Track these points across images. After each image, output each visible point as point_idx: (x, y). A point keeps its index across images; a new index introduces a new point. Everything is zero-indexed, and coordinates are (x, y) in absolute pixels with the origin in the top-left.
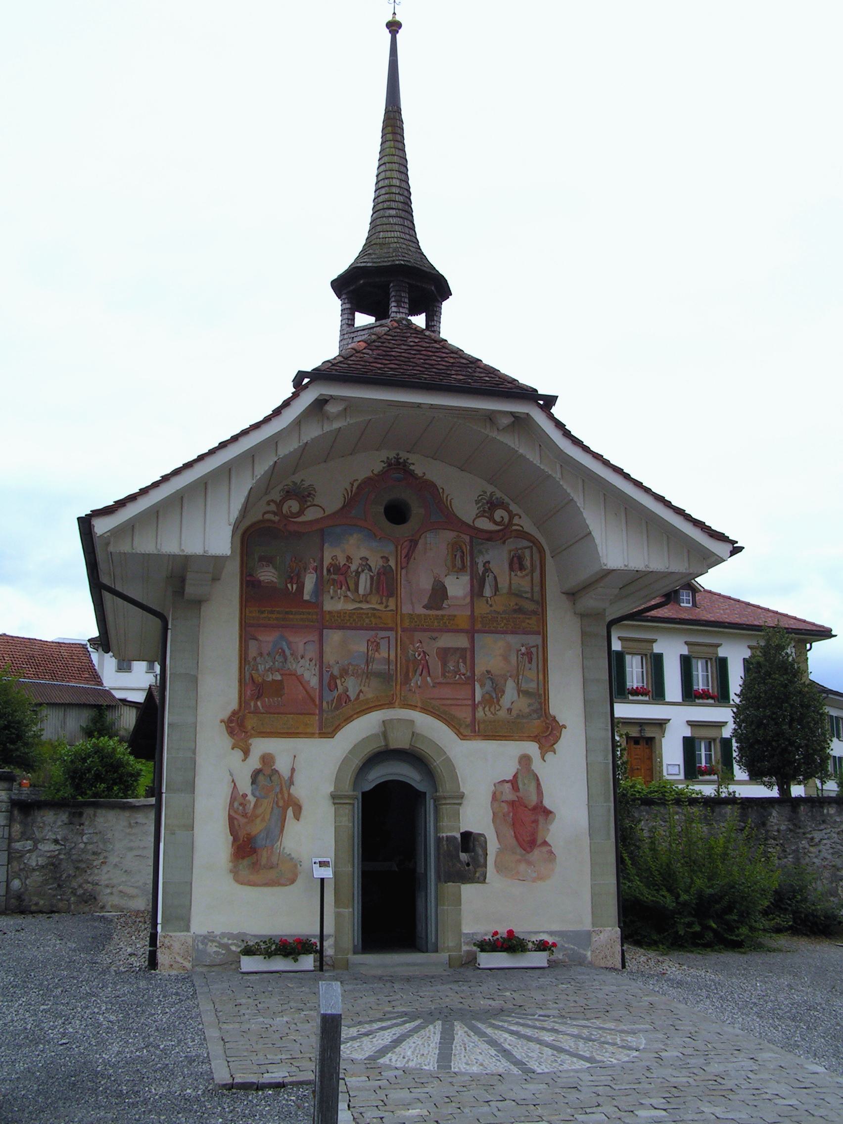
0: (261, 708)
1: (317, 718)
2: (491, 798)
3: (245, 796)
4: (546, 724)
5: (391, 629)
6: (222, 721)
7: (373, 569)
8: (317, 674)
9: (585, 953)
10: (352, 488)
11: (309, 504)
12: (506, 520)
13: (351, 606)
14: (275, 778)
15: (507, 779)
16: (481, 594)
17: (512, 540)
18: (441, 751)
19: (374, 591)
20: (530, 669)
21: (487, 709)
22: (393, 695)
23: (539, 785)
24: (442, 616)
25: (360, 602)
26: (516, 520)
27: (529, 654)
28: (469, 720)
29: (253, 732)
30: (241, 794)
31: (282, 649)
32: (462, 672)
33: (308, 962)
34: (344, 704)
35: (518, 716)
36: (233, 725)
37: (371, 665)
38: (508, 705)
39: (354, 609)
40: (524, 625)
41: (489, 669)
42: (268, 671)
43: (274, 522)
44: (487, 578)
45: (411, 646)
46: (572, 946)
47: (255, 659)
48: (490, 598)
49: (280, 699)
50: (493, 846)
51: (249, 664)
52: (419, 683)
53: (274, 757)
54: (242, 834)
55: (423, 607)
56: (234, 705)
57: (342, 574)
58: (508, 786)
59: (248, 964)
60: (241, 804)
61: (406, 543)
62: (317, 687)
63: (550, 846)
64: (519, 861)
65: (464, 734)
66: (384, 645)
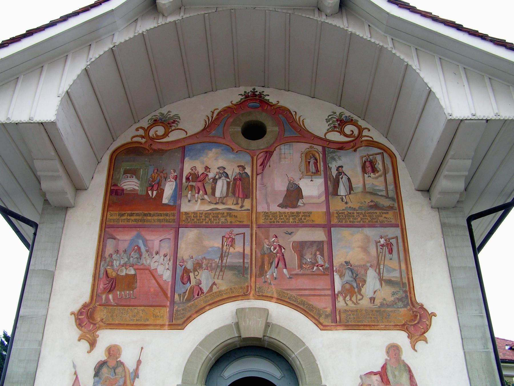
0: (112, 301)
1: (168, 310)
4: (413, 312)
5: (246, 226)
6: (72, 313)
7: (230, 176)
8: (171, 268)
10: (213, 114)
11: (173, 128)
12: (356, 132)
13: (207, 208)
14: (119, 370)
15: (375, 371)
16: (335, 193)
17: (362, 148)
18: (299, 342)
19: (230, 194)
20: (391, 259)
21: (348, 298)
22: (248, 286)
24: (298, 213)
25: (217, 203)
26: (365, 133)
28: (329, 310)
29: (101, 323)
31: (137, 246)
32: (319, 263)
34: (196, 296)
35: (382, 305)
36: (83, 317)
37: (225, 258)
38: (371, 295)
39: (211, 210)
40: (381, 219)
41: (348, 260)
42: (123, 266)
43: (140, 143)
44: (340, 179)
47: (111, 256)
48: (345, 196)
49: (132, 292)
51: (105, 260)
53: (121, 348)
56: (86, 298)
57: (200, 181)
58: (377, 377)
61: (262, 154)
62: (170, 280)
65: (324, 324)
66: (239, 241)
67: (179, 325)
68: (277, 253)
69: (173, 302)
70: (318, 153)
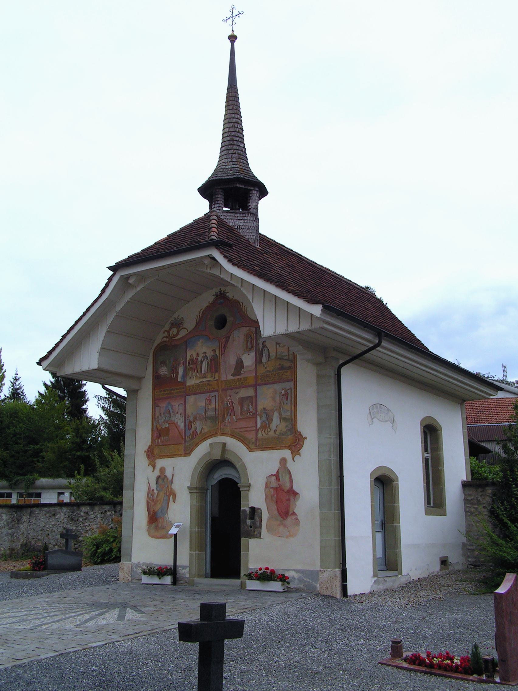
2: (264, 486)
3: (153, 490)
5: (216, 391)
8: (183, 421)
9: (316, 585)
10: (200, 314)
11: (181, 328)
14: (165, 480)
15: (273, 474)
18: (240, 459)
20: (287, 404)
21: (263, 431)
23: (290, 477)
27: (286, 395)
28: (254, 439)
30: (152, 489)
31: (169, 410)
33: (168, 580)
35: (280, 434)
38: (275, 428)
40: (284, 376)
41: (264, 407)
43: (165, 342)
44: (264, 351)
45: (226, 399)
46: (308, 580)
47: (158, 417)
50: (265, 516)
52: (229, 420)
54: (152, 510)
55: (232, 375)
56: (149, 443)
57: (194, 364)
58: (274, 478)
59: (145, 579)
60: (152, 495)
62: (183, 428)
63: (296, 515)
64: (279, 525)
65: (251, 448)
67: (188, 454)
68: (231, 406)
69: (185, 441)
70: (253, 333)
